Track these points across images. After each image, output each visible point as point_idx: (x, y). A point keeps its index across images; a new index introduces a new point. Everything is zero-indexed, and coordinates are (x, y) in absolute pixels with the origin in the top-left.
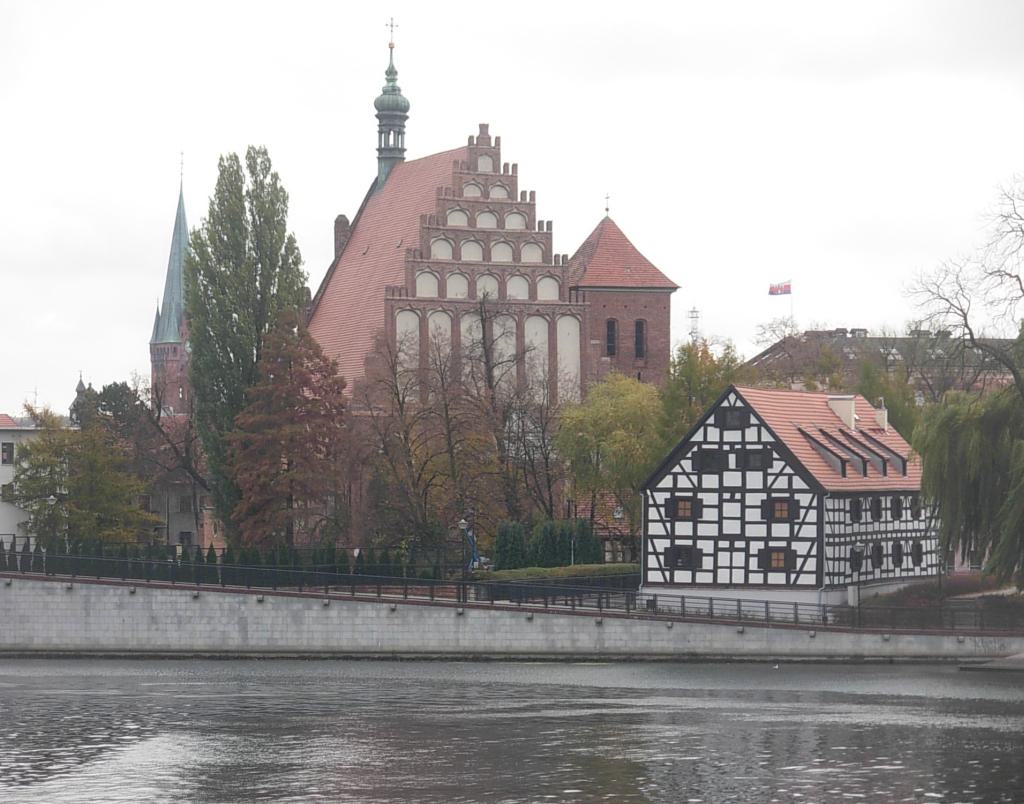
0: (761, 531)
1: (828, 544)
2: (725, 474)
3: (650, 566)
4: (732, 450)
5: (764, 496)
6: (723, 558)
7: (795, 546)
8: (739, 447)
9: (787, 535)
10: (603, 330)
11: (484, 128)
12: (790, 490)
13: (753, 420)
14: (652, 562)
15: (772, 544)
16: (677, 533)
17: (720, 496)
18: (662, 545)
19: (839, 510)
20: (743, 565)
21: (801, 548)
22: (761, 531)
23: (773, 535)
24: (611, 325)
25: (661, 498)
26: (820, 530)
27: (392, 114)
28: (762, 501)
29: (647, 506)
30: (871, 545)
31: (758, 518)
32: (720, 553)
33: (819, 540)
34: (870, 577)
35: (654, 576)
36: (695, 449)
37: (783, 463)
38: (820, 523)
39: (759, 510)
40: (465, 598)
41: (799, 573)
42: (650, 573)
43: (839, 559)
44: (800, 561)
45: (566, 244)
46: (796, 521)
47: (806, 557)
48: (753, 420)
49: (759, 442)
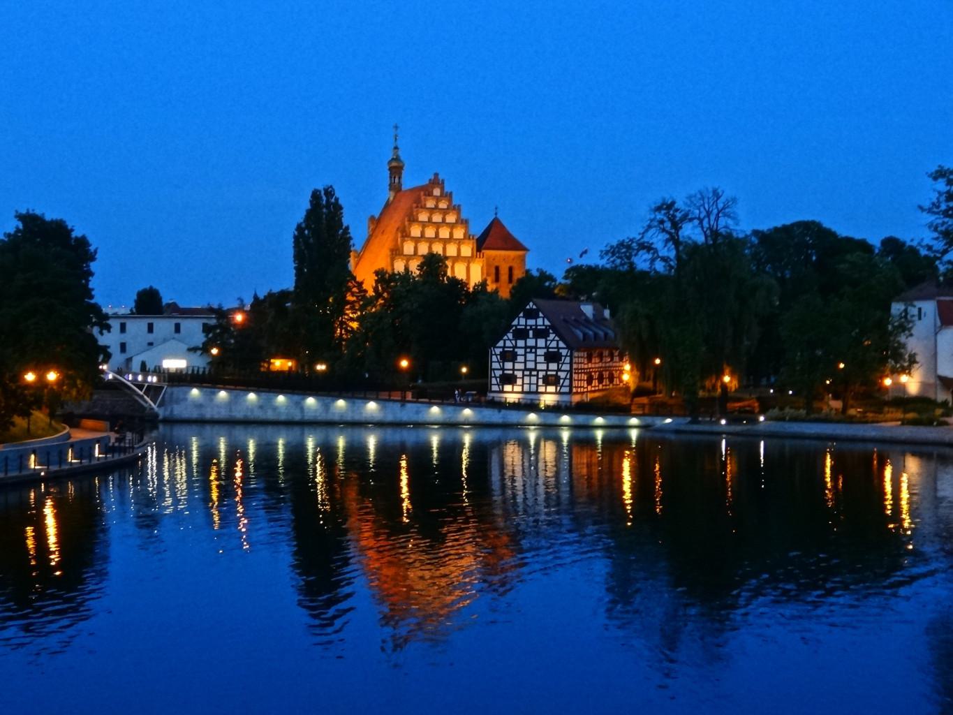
0: (544, 367)
1: (575, 373)
2: (528, 340)
3: (493, 383)
4: (531, 329)
5: (545, 350)
6: (527, 380)
7: (559, 373)
8: (534, 327)
9: (556, 369)
10: (493, 271)
11: (436, 175)
12: (558, 347)
13: (541, 315)
14: (494, 381)
15: (549, 373)
16: (506, 367)
18: (498, 373)
19: (581, 357)
20: (535, 382)
21: (562, 375)
22: (544, 367)
23: (550, 369)
24: (497, 269)
25: (498, 351)
26: (571, 367)
27: (396, 170)
28: (545, 353)
29: (492, 355)
30: (597, 373)
31: (543, 361)
32: (525, 377)
33: (570, 371)
34: (597, 388)
35: (495, 388)
36: (514, 328)
37: (554, 335)
38: (571, 364)
39: (543, 358)
40: (405, 398)
42: (493, 386)
43: (581, 380)
44: (561, 381)
45: (478, 229)
48: (541, 315)
49: (544, 325)
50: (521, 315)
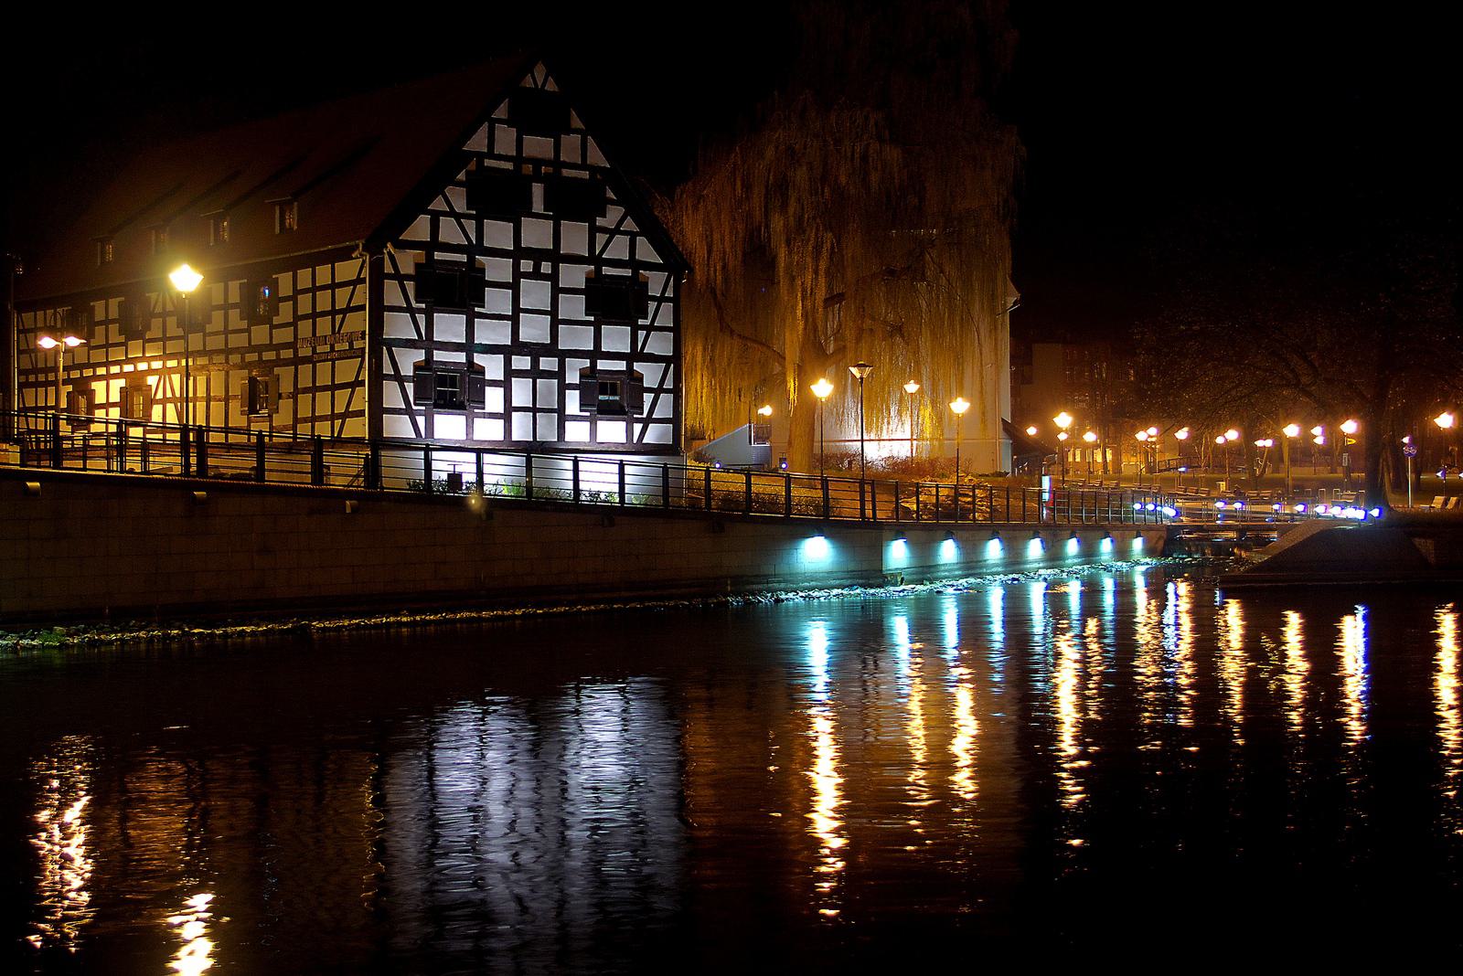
4: (537, 177)
7: (637, 366)
12: (633, 263)
14: (392, 396)
15: (602, 365)
17: (516, 266)
18: (408, 361)
21: (650, 374)
25: (408, 262)
32: (516, 383)
36: (472, 166)
41: (646, 422)
46: (640, 322)
47: (658, 392)
48: (577, 123)
50: (501, 112)
